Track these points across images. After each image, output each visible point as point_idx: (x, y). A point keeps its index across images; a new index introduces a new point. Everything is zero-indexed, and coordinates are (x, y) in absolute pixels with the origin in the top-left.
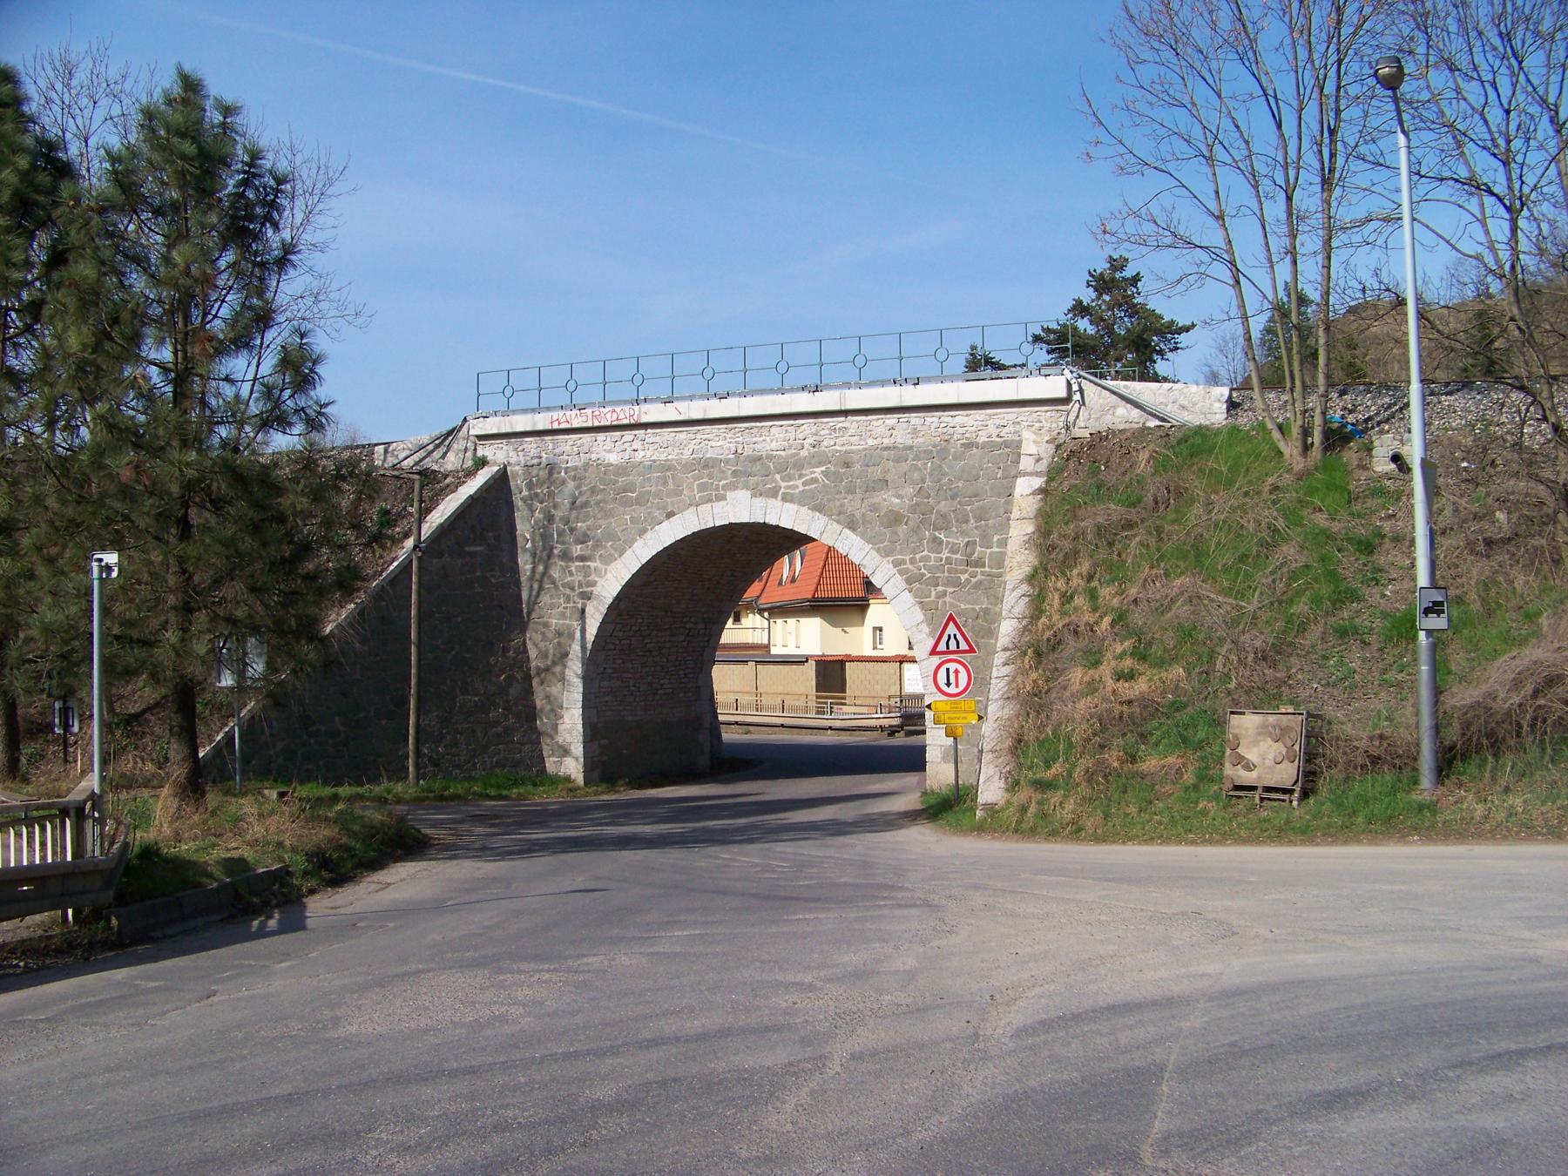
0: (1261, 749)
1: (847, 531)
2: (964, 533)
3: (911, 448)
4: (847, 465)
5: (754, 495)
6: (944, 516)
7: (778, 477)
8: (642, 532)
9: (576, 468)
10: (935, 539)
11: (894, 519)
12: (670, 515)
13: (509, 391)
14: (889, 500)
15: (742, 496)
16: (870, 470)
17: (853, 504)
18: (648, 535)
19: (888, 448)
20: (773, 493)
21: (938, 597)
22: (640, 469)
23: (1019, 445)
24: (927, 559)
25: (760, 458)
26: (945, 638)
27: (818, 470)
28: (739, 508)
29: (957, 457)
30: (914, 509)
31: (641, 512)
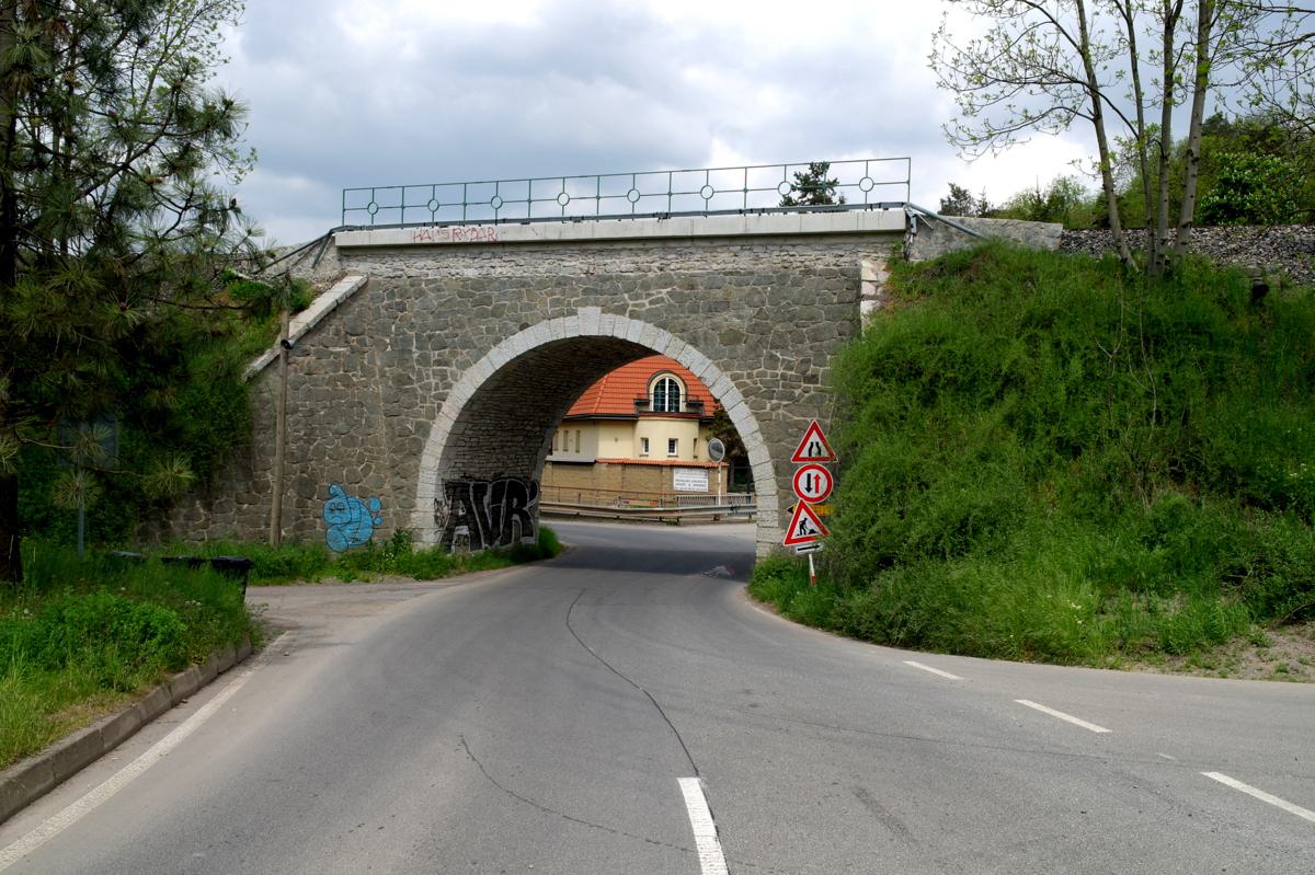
0: (439, 514)
1: (690, 347)
2: (798, 353)
3: (752, 273)
4: (692, 287)
5: (603, 312)
6: (781, 336)
7: (626, 296)
8: (497, 341)
9: (435, 281)
10: (772, 357)
11: (733, 338)
12: (524, 327)
13: (373, 207)
14: (730, 320)
15: (592, 312)
16: (713, 291)
17: (701, 324)
18: (503, 344)
19: (731, 273)
20: (621, 310)
21: (772, 409)
22: (496, 284)
23: (857, 273)
24: (763, 374)
25: (611, 278)
26: (808, 445)
27: (664, 291)
28: (591, 322)
29: (796, 283)
30: (753, 329)
31: (496, 323)
